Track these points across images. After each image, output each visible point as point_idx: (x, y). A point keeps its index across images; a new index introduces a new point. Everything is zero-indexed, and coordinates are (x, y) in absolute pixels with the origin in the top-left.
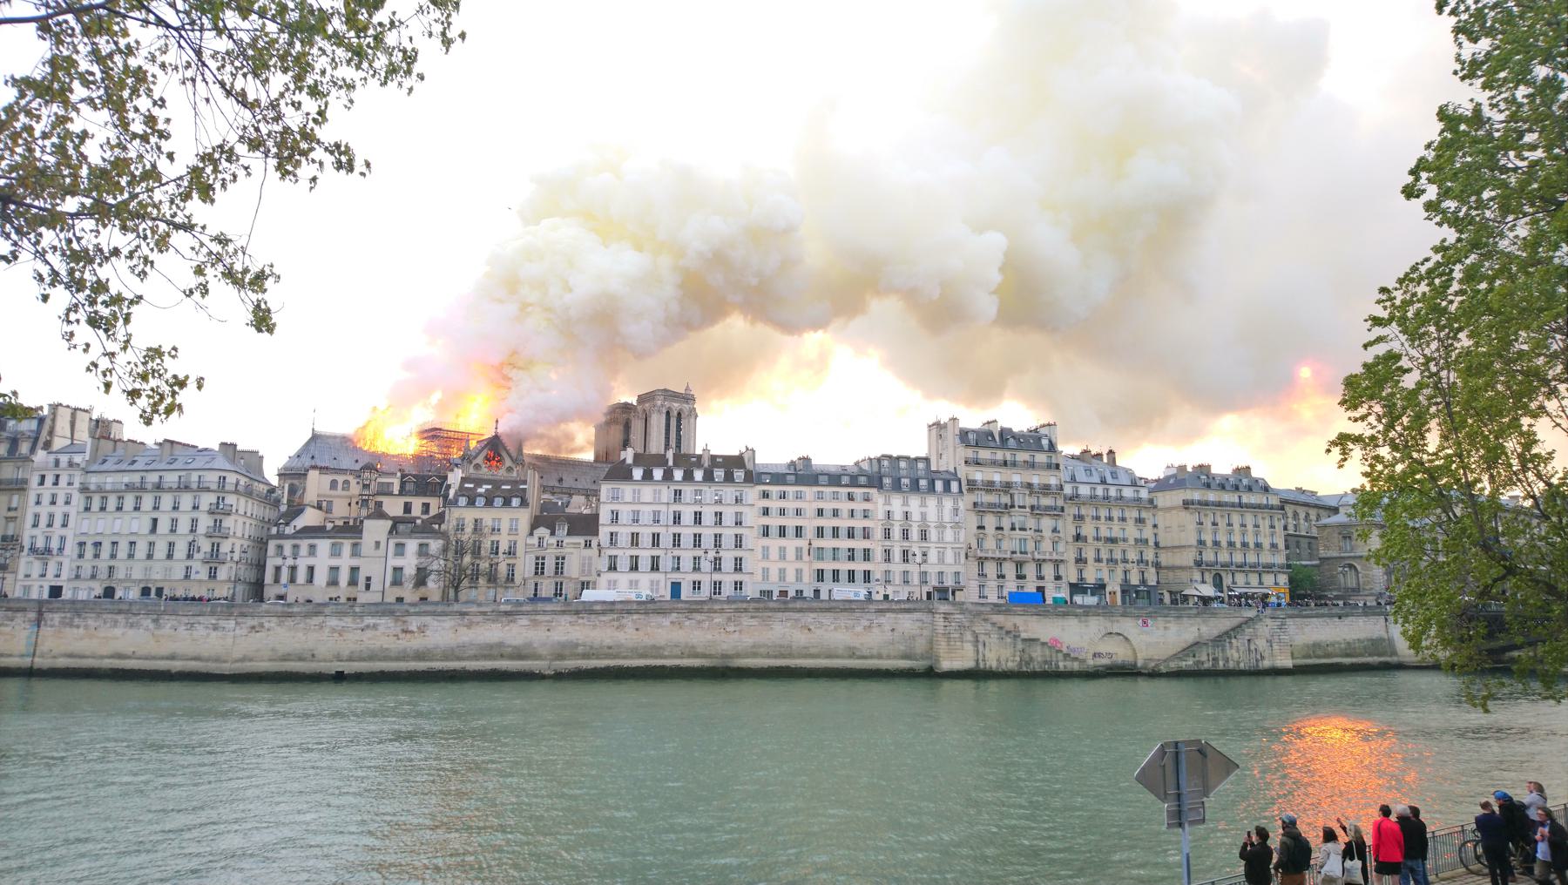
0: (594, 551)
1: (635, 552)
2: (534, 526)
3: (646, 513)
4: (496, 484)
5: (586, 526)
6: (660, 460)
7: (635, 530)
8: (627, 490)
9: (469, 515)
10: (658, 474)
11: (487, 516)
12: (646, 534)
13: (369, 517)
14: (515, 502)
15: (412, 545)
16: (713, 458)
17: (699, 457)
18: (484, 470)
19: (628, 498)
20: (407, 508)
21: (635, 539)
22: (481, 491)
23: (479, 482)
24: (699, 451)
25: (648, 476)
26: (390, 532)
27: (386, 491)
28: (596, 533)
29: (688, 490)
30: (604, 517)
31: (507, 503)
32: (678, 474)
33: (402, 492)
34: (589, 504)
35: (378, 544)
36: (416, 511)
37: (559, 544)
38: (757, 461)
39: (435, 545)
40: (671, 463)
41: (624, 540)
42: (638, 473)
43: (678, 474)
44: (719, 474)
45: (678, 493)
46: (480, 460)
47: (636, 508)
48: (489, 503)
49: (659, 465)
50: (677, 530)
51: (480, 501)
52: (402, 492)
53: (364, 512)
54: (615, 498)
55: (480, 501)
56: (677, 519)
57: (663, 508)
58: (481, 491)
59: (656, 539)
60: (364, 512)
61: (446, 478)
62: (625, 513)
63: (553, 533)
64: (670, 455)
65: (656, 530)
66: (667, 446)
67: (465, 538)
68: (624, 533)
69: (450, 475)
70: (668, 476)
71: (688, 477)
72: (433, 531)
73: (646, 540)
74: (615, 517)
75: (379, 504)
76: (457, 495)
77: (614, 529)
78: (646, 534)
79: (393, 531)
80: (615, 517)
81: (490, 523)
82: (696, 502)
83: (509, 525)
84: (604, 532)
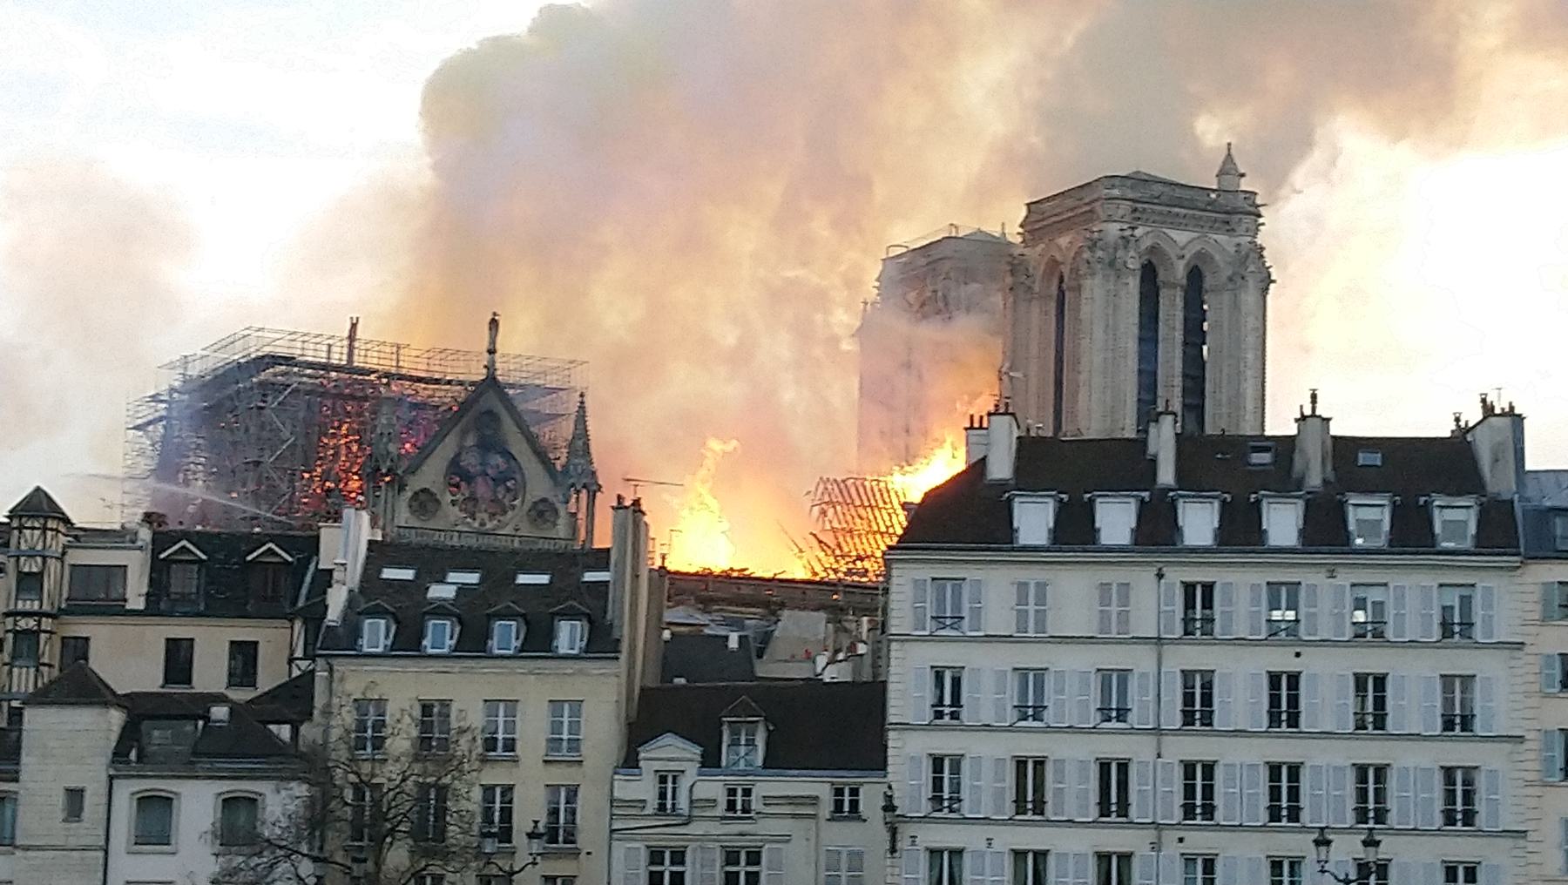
0: (869, 834)
1: (1030, 838)
2: (643, 724)
3: (1073, 674)
4: (497, 566)
5: (836, 729)
6: (1122, 464)
7: (1030, 746)
8: (993, 587)
9: (402, 689)
10: (1116, 519)
11: (468, 692)
12: (1073, 762)
13: (42, 697)
14: (568, 635)
15: (198, 803)
16: (1347, 448)
17: (1286, 444)
18: (451, 514)
19: (998, 619)
20: (178, 659)
21: (1030, 788)
22: (441, 592)
23: (433, 562)
24: (1280, 423)
25: (1075, 531)
26: (119, 755)
27: (96, 596)
28: (877, 762)
29: (1240, 587)
30: (907, 696)
31: (538, 642)
32: (1199, 521)
33: (159, 603)
34: (843, 648)
35: (75, 797)
36: (210, 673)
37: (737, 805)
38: (1530, 465)
39: (280, 803)
40: (1166, 475)
41: (988, 786)
42: (1034, 519)
43: (1199, 521)
44: (1369, 515)
45: (1199, 597)
46: (431, 475)
47: (1031, 657)
48: (473, 643)
49: (1117, 485)
50: (1197, 748)
51: (440, 635)
52: (159, 603)
53: (24, 680)
54: (948, 620)
55: (440, 635)
56: (1198, 704)
57: (1140, 660)
58: (441, 592)
59: (1113, 787)
60: (24, 680)
61: (313, 545)
62: (989, 677)
63: (710, 761)
64: (1163, 441)
65: (1114, 747)
66: (1148, 413)
67: (388, 774)
68: (987, 760)
69: (329, 536)
70: (1157, 530)
71: (1240, 532)
72: (275, 750)
73: (1073, 790)
74: (949, 694)
75: (77, 649)
76: (356, 611)
77: (946, 743)
78: (1073, 762)
79: (129, 752)
80: (949, 694)
81: (477, 719)
82: (1276, 634)
83: (548, 718)
84: (908, 754)
